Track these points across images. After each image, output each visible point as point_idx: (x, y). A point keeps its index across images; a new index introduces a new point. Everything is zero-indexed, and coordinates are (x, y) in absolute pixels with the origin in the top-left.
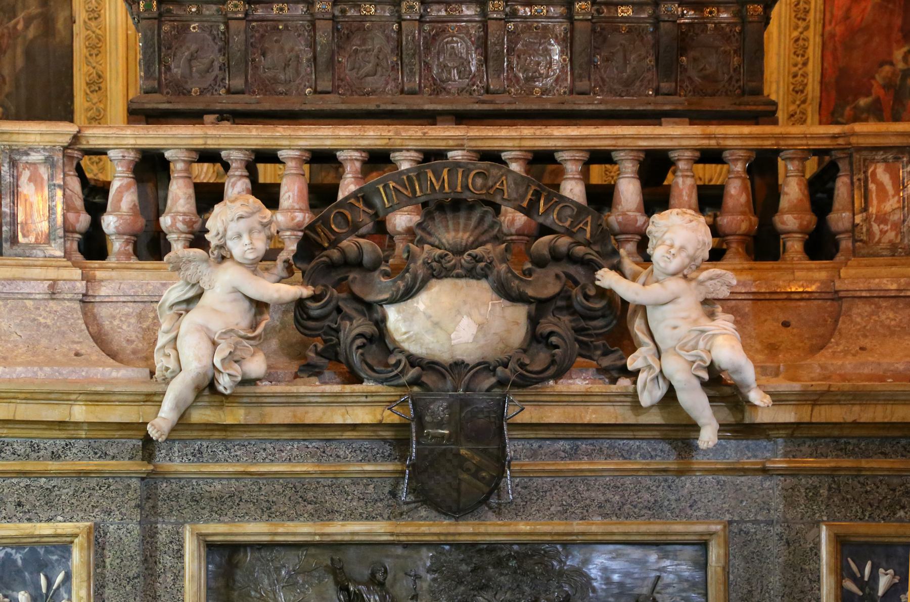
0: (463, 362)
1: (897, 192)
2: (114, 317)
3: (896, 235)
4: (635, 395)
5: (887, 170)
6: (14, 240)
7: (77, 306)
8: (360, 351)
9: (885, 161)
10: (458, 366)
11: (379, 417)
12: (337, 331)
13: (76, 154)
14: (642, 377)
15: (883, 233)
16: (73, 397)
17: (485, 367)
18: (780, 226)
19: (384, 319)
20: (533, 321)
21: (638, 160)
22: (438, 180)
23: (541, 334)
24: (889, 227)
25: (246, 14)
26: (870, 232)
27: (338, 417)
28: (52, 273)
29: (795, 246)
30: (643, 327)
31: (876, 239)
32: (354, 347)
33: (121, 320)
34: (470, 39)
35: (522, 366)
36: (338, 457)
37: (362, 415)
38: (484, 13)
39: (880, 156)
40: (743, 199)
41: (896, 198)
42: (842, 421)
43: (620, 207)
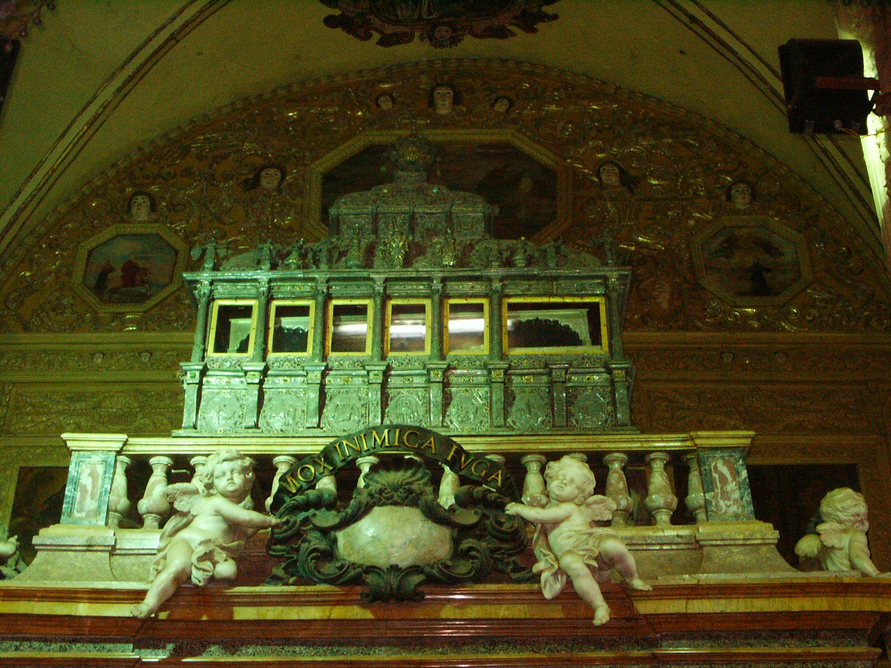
0: (397, 566)
1: (734, 479)
2: (134, 565)
3: (738, 508)
4: (540, 592)
5: (726, 463)
6: (70, 514)
7: (107, 555)
8: (313, 561)
9: (722, 458)
10: (394, 568)
11: (328, 614)
12: (297, 550)
13: (126, 460)
14: (544, 576)
15: (728, 506)
16: (80, 595)
17: (414, 569)
18: (650, 504)
19: (335, 541)
20: (456, 541)
21: (540, 462)
22: (380, 439)
23: (462, 550)
24: (732, 502)
25: (261, 382)
26: (717, 505)
27: (294, 613)
28: (92, 533)
29: (664, 517)
30: (544, 543)
31: (723, 511)
32: (309, 558)
33: (139, 567)
34: (419, 397)
35: (447, 567)
36: (295, 652)
37: (313, 613)
38: (429, 381)
39: (718, 454)
40: (621, 485)
41: (734, 483)
42: (712, 611)
43: (528, 493)
